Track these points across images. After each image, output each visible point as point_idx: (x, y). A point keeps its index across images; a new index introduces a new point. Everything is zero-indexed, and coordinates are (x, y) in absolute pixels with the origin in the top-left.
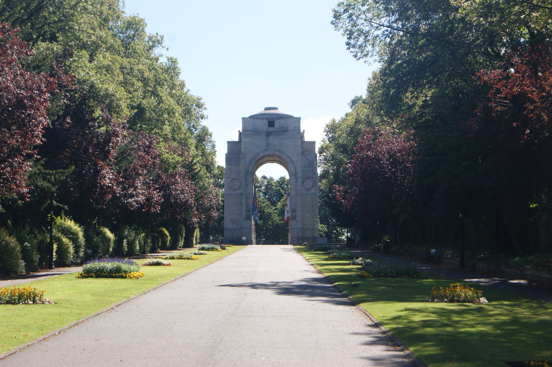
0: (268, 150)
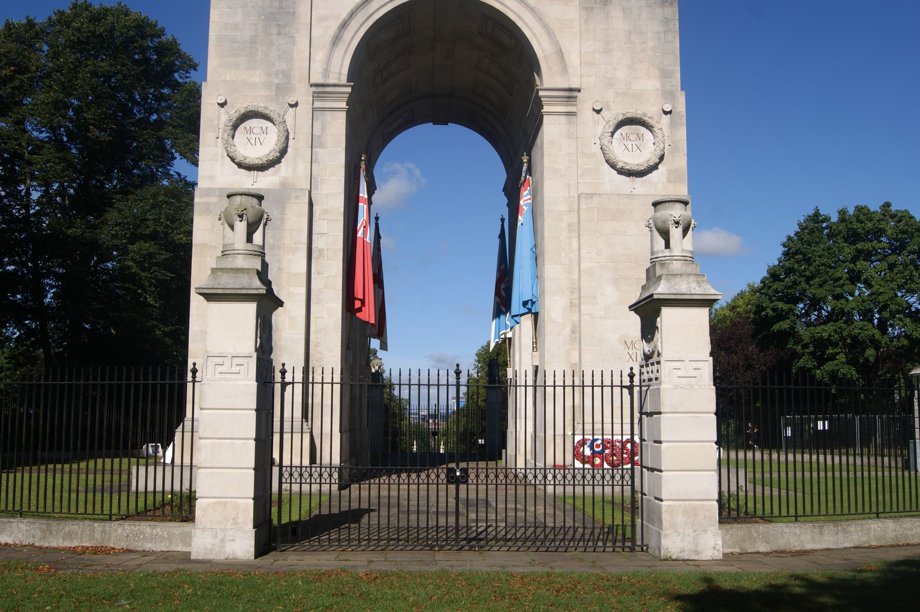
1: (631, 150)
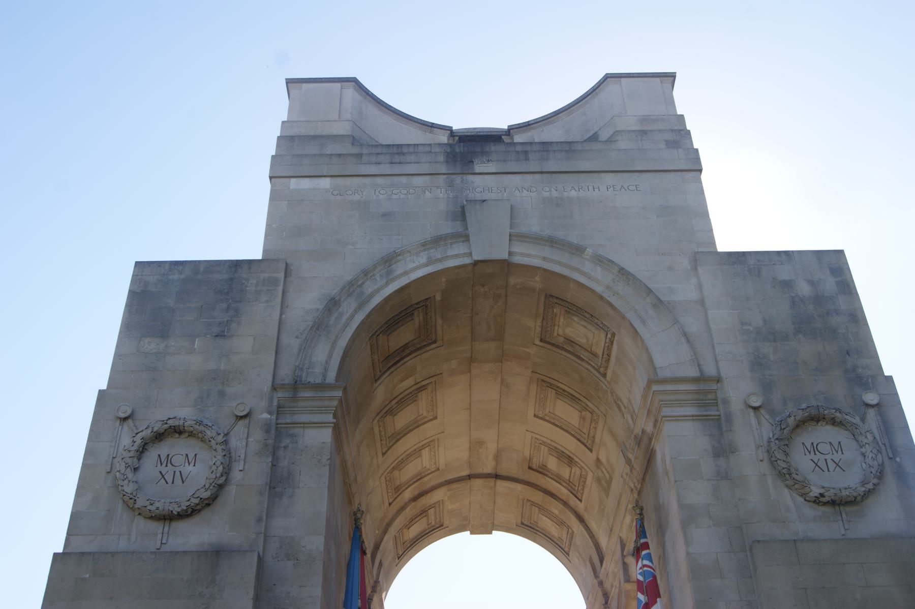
0: (463, 237)
1: (825, 469)
